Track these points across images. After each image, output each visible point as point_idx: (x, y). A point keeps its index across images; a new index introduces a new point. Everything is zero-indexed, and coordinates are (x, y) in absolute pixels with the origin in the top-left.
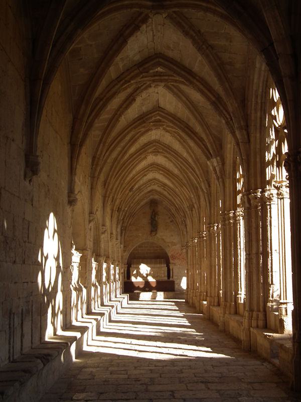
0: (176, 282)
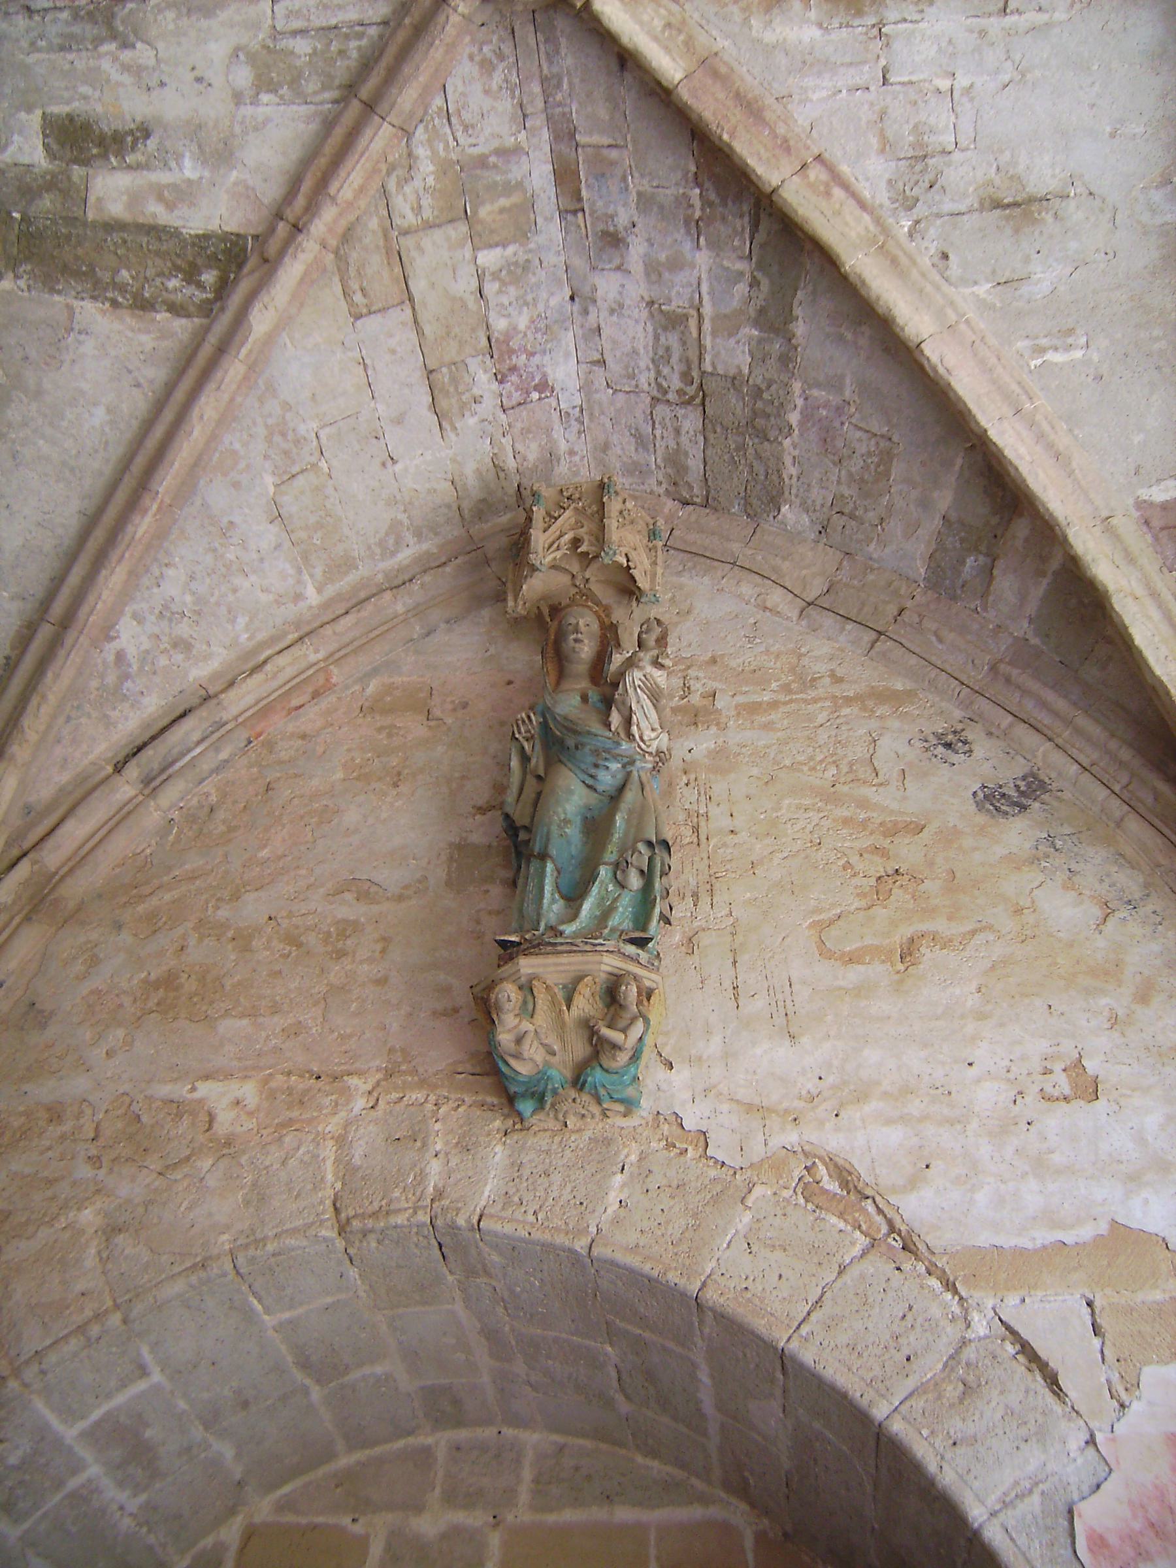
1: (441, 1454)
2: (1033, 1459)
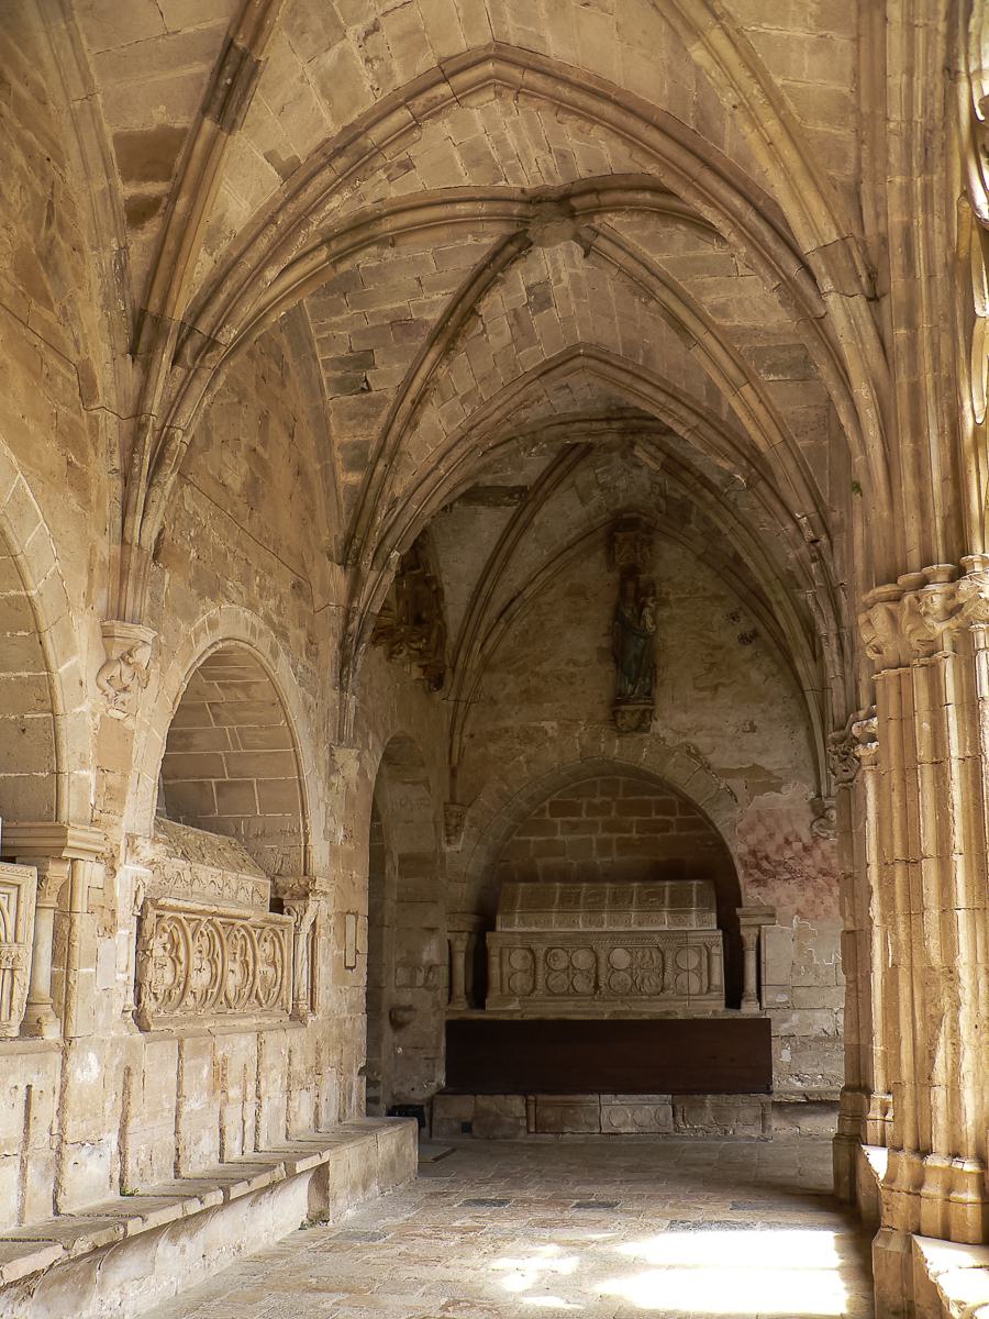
0: (779, 1029)
2: (730, 815)
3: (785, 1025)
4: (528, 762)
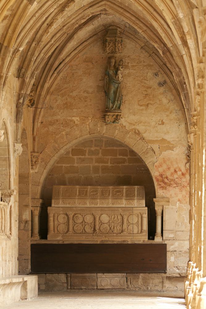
0: (169, 248)
1: (94, 141)
2: (152, 159)
3: (172, 247)
4: (67, 135)
